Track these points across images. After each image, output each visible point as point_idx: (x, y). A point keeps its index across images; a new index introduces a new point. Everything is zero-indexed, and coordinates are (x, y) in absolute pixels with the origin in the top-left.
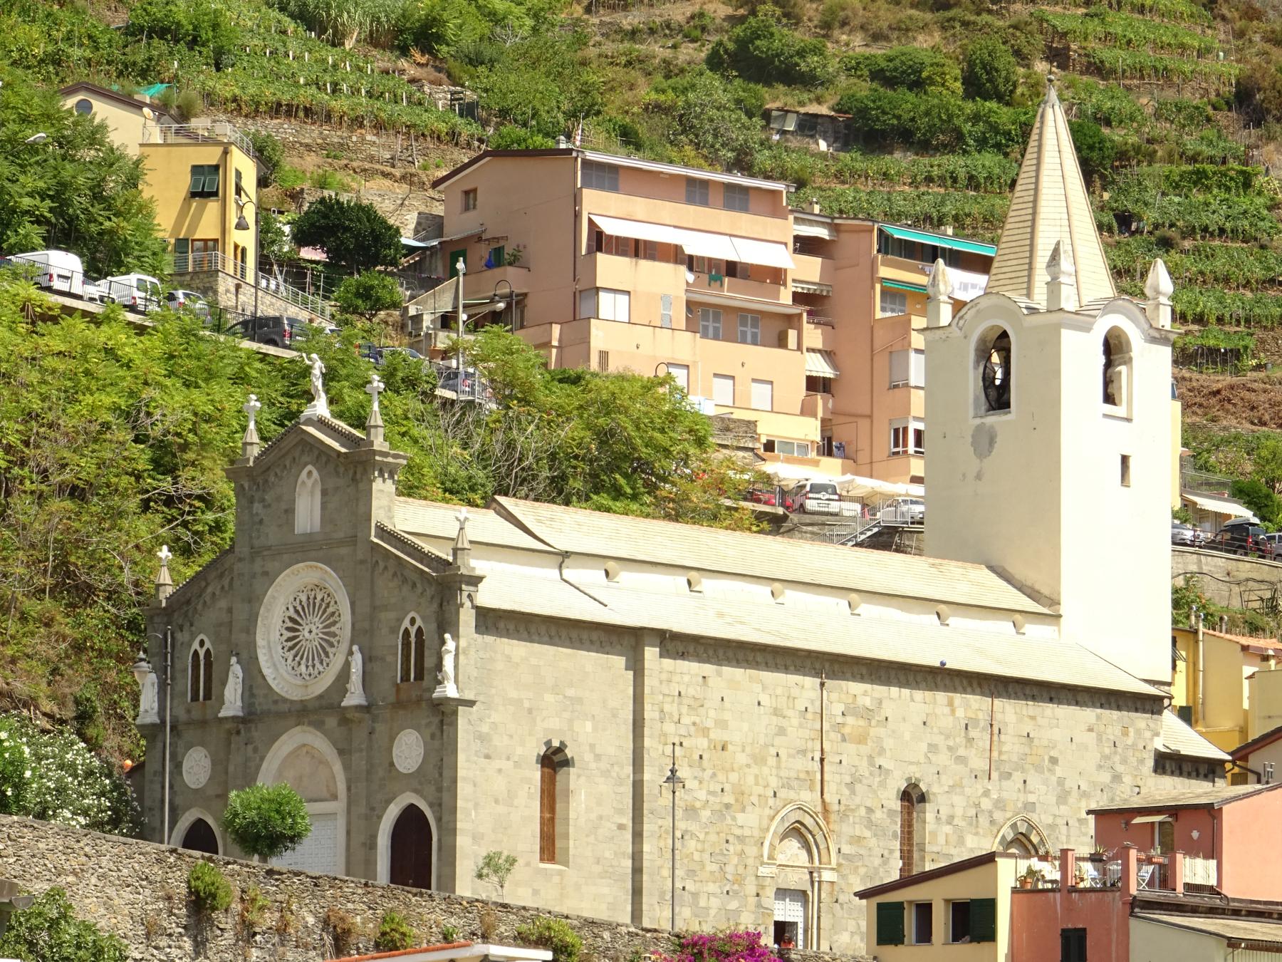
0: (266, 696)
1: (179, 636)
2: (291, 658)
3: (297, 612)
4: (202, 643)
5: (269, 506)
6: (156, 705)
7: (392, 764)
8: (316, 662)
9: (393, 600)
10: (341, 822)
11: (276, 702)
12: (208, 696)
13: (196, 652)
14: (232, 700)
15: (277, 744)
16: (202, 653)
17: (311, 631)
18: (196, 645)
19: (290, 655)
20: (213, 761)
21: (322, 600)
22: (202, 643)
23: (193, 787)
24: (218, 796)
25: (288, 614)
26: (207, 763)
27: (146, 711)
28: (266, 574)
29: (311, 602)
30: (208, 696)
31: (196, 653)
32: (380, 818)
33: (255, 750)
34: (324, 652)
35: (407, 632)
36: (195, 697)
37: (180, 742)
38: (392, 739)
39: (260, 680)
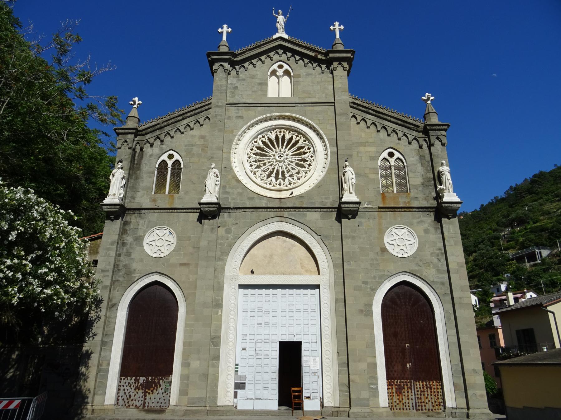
0: (240, 194)
1: (147, 149)
4: (171, 156)
5: (244, 80)
6: (122, 191)
7: (384, 250)
9: (370, 140)
16: (170, 163)
20: (180, 239)
22: (171, 156)
23: (155, 255)
24: (182, 264)
25: (256, 145)
27: (114, 195)
28: (242, 117)
32: (374, 290)
33: (228, 231)
37: (141, 222)
38: (382, 233)
39: (234, 183)
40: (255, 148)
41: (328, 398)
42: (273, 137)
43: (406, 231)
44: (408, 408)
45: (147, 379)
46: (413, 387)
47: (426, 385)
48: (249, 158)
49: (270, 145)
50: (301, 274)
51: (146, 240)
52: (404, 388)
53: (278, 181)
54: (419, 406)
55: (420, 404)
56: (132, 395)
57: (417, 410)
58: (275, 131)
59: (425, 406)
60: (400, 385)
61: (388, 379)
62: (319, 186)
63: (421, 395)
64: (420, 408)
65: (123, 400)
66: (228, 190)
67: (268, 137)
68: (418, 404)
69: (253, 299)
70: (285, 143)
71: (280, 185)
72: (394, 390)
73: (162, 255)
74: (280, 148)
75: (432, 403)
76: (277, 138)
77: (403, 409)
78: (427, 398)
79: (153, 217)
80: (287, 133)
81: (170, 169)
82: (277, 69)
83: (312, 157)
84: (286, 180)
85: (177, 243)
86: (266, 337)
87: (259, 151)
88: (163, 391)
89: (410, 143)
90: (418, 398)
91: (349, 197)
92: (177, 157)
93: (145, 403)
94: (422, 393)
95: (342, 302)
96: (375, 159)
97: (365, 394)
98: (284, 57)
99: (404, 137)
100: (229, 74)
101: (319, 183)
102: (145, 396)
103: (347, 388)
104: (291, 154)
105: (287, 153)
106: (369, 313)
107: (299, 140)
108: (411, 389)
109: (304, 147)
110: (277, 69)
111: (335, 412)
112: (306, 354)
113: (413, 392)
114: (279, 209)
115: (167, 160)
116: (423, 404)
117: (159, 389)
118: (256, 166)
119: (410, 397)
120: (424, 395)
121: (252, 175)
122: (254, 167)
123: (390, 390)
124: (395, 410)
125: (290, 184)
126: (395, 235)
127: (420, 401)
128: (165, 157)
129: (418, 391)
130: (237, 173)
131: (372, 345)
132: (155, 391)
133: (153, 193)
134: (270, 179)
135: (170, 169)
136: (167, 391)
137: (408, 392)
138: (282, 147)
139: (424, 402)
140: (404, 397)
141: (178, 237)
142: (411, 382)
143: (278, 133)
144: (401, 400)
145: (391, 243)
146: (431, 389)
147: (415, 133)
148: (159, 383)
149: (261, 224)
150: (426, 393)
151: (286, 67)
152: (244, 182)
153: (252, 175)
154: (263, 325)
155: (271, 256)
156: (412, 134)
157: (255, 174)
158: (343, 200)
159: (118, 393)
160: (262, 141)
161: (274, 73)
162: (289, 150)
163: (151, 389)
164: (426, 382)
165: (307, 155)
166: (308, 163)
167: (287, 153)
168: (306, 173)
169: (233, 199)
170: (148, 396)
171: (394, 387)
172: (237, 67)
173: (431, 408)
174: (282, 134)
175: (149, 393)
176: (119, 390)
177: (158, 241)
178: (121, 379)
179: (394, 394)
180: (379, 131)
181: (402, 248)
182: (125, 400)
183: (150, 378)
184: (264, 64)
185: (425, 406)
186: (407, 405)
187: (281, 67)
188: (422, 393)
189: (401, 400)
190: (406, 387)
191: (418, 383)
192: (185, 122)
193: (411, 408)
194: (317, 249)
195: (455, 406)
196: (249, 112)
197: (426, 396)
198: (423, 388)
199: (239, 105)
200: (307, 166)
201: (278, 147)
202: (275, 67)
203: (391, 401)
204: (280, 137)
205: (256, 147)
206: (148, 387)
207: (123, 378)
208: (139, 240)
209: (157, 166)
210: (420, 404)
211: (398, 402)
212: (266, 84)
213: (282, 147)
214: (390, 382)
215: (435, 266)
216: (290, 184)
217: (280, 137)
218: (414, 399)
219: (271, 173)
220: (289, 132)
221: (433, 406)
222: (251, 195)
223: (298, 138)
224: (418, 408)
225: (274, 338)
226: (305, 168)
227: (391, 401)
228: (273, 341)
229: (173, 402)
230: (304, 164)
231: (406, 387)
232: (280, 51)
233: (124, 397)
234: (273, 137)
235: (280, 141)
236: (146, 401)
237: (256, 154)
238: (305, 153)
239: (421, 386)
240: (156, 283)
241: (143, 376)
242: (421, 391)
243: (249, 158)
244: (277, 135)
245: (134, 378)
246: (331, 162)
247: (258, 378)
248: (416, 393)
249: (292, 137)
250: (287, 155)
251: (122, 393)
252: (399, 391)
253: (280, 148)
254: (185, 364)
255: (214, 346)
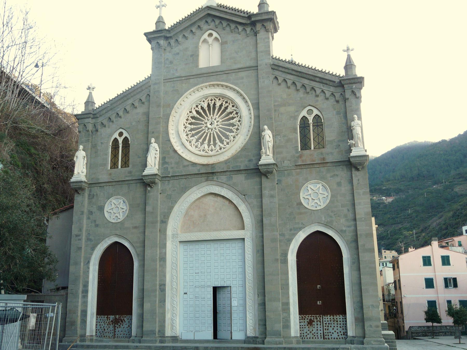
2: (195, 140)
3: (197, 112)
4: (121, 134)
6: (85, 170)
8: (217, 141)
10: (249, 245)
11: (184, 166)
12: (126, 164)
13: (116, 140)
14: (153, 165)
15: (187, 193)
16: (120, 140)
17: (214, 122)
18: (116, 135)
19: (194, 139)
21: (221, 106)
22: (121, 134)
23: (113, 221)
25: (191, 115)
26: (126, 207)
29: (211, 108)
30: (126, 164)
31: (116, 140)
32: (289, 241)
34: (222, 137)
35: (304, 119)
36: (114, 165)
39: (172, 153)
40: (190, 118)
41: (251, 330)
42: (205, 106)
43: (320, 185)
44: (317, 337)
45: (115, 317)
46: (321, 321)
47: (333, 319)
48: (185, 128)
49: (203, 113)
50: (231, 230)
51: (107, 208)
52: (314, 321)
53: (210, 147)
54: (326, 335)
55: (327, 334)
56: (106, 329)
57: (324, 338)
58: (207, 100)
59: (331, 335)
60: (311, 319)
61: (300, 313)
62: (244, 149)
63: (328, 326)
64: (327, 337)
65: (101, 333)
66: (167, 160)
67: (201, 106)
68: (325, 334)
69: (191, 253)
70: (216, 110)
71: (212, 150)
72: (306, 323)
73: (119, 221)
74: (212, 115)
75: (338, 333)
76: (209, 106)
77: (313, 338)
78: (333, 329)
79: (110, 189)
80: (218, 100)
81: (121, 146)
82: (207, 38)
83: (239, 121)
84: (217, 146)
85: (129, 209)
86: (203, 283)
87: (193, 121)
88: (127, 326)
89: (327, 99)
90: (325, 329)
91: (267, 158)
92: (125, 134)
93: (115, 335)
94: (329, 325)
95: (261, 251)
96: (295, 118)
97: (279, 327)
98: (212, 25)
99: (322, 94)
100: (165, 50)
101: (244, 146)
102: (115, 329)
103: (263, 322)
104: (221, 120)
105: (217, 120)
106: (285, 261)
107: (228, 106)
108: (320, 322)
109: (233, 112)
110: (207, 38)
111: (253, 340)
112: (234, 296)
113: (322, 324)
114: (209, 173)
115: (118, 137)
116: (330, 334)
117: (124, 324)
118: (191, 135)
119: (317, 328)
120: (331, 326)
121: (187, 144)
122: (189, 136)
123: (302, 324)
124: (306, 339)
125: (221, 149)
126: (310, 189)
127: (327, 331)
128: (116, 135)
129: (326, 324)
130: (174, 144)
131: (286, 286)
132: (121, 326)
133: (109, 168)
134: (203, 146)
135: (121, 146)
136: (130, 326)
137: (317, 324)
138: (213, 114)
139: (330, 332)
140: (314, 329)
141: (130, 205)
142: (320, 317)
143: (210, 102)
144: (311, 330)
145: (306, 197)
146: (337, 321)
147: (332, 89)
148: (124, 319)
149: (194, 188)
150: (333, 325)
151: (215, 35)
152: (180, 152)
153: (187, 144)
154: (200, 274)
155: (205, 215)
156: (328, 90)
157: (190, 142)
158: (260, 163)
159: (96, 327)
160: (196, 111)
161: (205, 41)
162: (219, 117)
163: (119, 324)
164: (333, 316)
165: (235, 120)
166: (236, 127)
167: (217, 120)
168: (234, 137)
169: (172, 168)
170: (117, 330)
171: (306, 320)
172: (172, 41)
173: (336, 338)
174: (213, 102)
175: (118, 328)
176: (96, 325)
177: (116, 209)
178: (97, 317)
179: (307, 327)
180: (299, 90)
181: (316, 201)
182: (101, 332)
183: (117, 316)
184: (195, 35)
185: (331, 335)
186: (316, 335)
187: (210, 35)
188: (329, 325)
189: (311, 330)
190: (315, 320)
191: (326, 317)
192: (130, 102)
193: (320, 337)
194: (242, 208)
195: (354, 335)
196: (184, 85)
197: (332, 327)
198: (330, 321)
199: (172, 80)
200: (235, 131)
201: (210, 115)
202: (205, 36)
203: (302, 332)
204: (212, 105)
205: (191, 117)
206: (116, 322)
207: (98, 316)
208: (101, 209)
209: (111, 144)
210: (327, 334)
211: (308, 332)
212: (198, 56)
213: (213, 114)
214: (302, 317)
215: (346, 216)
216: (221, 149)
217: (212, 105)
218: (322, 330)
219: (204, 140)
220: (219, 100)
221: (338, 336)
222: (186, 163)
223: (227, 104)
224: (325, 337)
225: (209, 284)
226: (233, 132)
227: (302, 332)
228: (208, 286)
229: (134, 333)
230: (233, 128)
231: (315, 320)
232: (209, 20)
233: (100, 330)
234: (205, 106)
235: (211, 108)
236: (116, 333)
237: (191, 124)
238: (233, 118)
239: (329, 320)
240: (116, 243)
241: (112, 315)
242: (329, 324)
243: (185, 128)
244: (208, 103)
245: (106, 316)
246: (254, 126)
247: (197, 315)
248: (324, 325)
249: (222, 103)
250: (217, 122)
251: (98, 326)
252: (310, 323)
253: (212, 115)
254: (141, 305)
255: (161, 291)
